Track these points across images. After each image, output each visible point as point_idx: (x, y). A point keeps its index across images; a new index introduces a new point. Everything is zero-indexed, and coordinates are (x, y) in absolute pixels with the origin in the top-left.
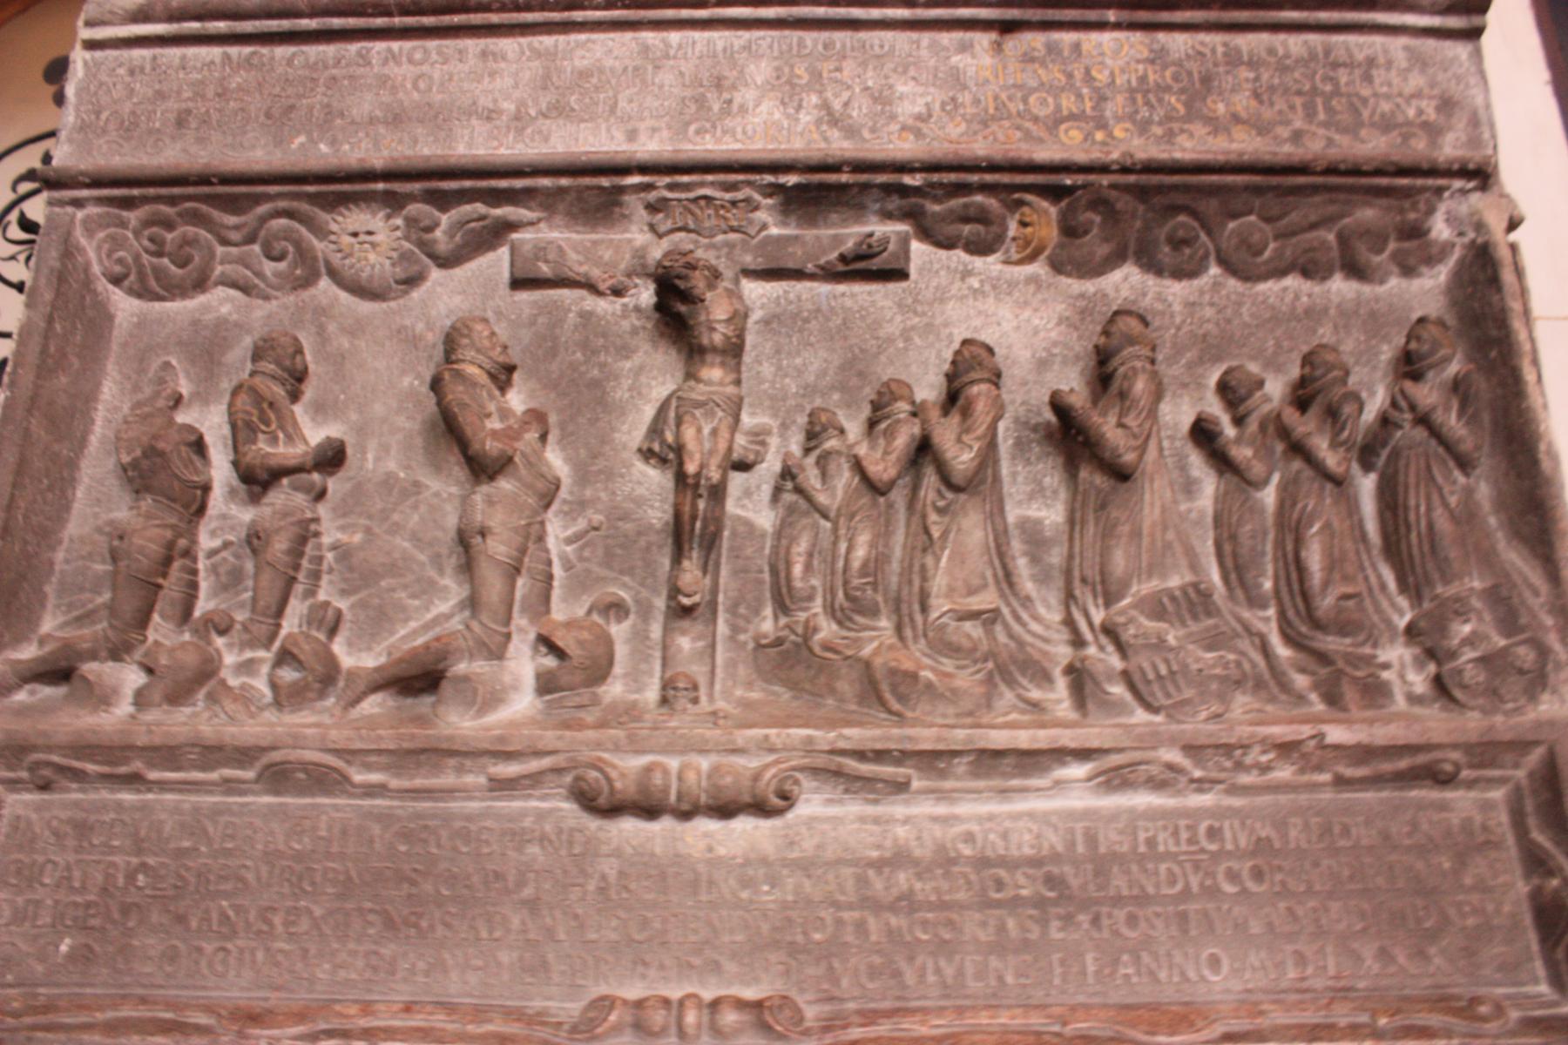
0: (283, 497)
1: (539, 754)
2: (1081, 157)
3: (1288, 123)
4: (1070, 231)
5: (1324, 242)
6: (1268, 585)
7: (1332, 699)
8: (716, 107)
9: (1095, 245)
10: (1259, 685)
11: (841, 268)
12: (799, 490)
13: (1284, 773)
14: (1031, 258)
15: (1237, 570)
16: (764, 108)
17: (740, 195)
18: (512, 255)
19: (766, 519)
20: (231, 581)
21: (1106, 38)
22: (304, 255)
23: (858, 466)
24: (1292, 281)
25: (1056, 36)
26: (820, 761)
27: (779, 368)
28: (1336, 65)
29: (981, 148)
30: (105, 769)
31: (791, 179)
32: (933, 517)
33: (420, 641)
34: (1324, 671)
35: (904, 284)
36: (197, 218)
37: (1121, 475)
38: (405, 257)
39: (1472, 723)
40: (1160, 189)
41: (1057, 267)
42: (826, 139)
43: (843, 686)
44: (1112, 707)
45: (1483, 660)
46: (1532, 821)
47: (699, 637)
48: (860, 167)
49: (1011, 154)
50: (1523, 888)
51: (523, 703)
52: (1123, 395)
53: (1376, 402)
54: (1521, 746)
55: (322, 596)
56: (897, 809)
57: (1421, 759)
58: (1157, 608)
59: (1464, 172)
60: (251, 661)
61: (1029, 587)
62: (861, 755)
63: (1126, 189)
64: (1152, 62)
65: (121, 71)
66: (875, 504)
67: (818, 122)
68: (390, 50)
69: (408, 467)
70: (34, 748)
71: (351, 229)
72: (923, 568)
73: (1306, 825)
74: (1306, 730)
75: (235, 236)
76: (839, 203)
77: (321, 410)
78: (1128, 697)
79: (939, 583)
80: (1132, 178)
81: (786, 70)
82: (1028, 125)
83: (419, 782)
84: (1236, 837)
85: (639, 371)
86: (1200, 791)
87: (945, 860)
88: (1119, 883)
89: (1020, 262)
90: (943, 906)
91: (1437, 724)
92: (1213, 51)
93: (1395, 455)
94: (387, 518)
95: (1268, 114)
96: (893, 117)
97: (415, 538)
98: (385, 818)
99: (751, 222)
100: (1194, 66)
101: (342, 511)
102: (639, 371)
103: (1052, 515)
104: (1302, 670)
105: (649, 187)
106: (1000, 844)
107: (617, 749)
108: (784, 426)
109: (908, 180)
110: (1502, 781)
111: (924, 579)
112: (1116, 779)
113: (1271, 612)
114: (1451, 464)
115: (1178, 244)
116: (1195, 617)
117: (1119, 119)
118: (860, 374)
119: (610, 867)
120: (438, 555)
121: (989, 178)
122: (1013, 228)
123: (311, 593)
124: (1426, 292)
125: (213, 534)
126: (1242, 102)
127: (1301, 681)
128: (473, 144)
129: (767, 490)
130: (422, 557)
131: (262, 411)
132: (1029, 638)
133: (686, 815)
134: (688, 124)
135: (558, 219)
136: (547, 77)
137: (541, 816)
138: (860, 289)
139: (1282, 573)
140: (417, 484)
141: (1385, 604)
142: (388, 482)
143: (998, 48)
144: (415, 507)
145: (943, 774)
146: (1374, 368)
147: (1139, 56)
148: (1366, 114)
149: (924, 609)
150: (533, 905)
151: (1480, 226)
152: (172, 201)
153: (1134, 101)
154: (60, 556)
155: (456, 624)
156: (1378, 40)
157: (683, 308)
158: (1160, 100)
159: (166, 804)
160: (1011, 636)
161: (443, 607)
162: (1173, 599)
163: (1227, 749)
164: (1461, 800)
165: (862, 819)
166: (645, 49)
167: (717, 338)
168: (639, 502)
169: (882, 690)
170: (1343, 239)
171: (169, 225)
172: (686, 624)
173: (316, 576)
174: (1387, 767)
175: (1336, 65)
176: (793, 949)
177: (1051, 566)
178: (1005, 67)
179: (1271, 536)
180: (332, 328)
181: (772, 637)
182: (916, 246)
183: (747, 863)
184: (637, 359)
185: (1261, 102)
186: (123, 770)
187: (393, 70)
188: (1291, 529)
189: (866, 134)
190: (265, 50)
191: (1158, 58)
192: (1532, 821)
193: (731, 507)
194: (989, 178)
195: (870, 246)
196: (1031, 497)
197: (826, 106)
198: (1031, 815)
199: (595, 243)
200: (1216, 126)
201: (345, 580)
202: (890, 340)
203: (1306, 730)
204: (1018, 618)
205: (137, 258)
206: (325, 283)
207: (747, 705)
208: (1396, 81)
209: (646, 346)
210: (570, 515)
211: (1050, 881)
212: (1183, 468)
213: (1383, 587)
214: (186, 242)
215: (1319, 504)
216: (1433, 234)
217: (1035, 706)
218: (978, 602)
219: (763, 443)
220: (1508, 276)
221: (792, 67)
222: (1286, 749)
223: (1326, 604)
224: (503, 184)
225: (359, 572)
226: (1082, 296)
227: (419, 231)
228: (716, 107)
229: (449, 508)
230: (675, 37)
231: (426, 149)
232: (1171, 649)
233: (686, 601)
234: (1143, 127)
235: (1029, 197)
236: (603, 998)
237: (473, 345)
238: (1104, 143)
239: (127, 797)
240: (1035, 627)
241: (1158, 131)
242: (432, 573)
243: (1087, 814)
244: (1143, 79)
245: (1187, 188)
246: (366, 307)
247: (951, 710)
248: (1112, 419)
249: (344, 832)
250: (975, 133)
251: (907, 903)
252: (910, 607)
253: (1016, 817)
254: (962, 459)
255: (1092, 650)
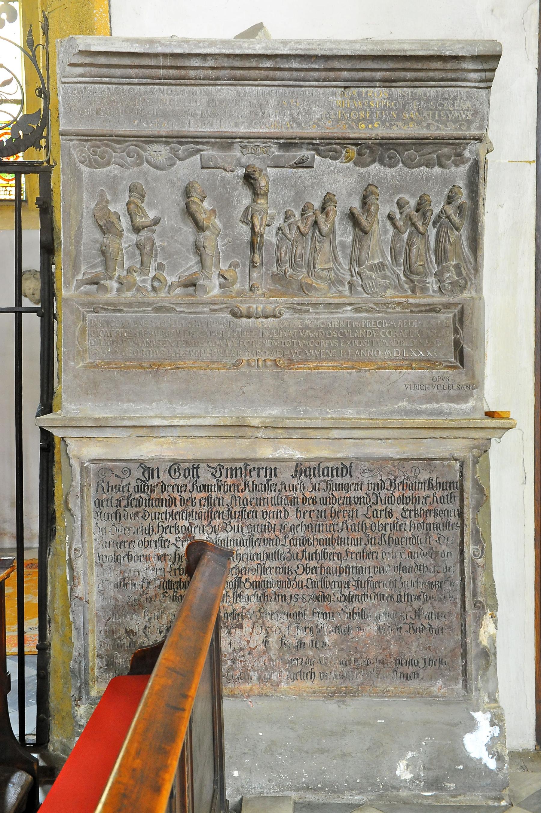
0: (144, 233)
1: (223, 304)
2: (363, 136)
3: (426, 121)
4: (360, 154)
5: (433, 158)
6: (402, 260)
7: (413, 291)
8: (260, 115)
9: (367, 157)
10: (395, 288)
11: (295, 166)
12: (282, 233)
13: (399, 309)
14: (349, 161)
15: (395, 257)
16: (274, 115)
17: (267, 145)
18: (201, 159)
19: (274, 240)
20: (132, 256)
21: (376, 89)
22: (139, 156)
23: (298, 228)
24: (423, 168)
25: (361, 89)
26: (289, 306)
27: (278, 195)
28: (445, 99)
29: (337, 132)
30: (114, 308)
31: (282, 141)
32: (317, 243)
33: (186, 274)
34: (412, 285)
35: (312, 169)
36: (107, 145)
37: (366, 233)
38: (170, 158)
39: (445, 300)
40: (385, 144)
41: (356, 164)
42: (292, 127)
43: (294, 286)
44: (358, 293)
45: (450, 283)
46: (457, 322)
47: (259, 273)
48: (301, 138)
49: (344, 135)
50: (453, 338)
51: (216, 291)
52: (368, 210)
53: (437, 210)
54: (457, 304)
55: (159, 261)
56: (307, 316)
57: (431, 307)
58: (371, 268)
59: (474, 139)
60: (145, 279)
61: (341, 260)
62: (298, 304)
63: (377, 144)
64: (389, 99)
65: (75, 92)
66: (303, 239)
67: (290, 121)
68: (160, 89)
69: (177, 223)
70: (95, 303)
71: (154, 150)
72: (314, 257)
73: (403, 321)
74: (404, 299)
75: (118, 151)
76: (295, 147)
77: (150, 205)
78: (362, 290)
79: (318, 260)
80: (378, 141)
81: (281, 102)
82: (350, 122)
83: (192, 310)
84: (386, 324)
85: (239, 195)
86: (378, 313)
87: (318, 328)
88: (357, 334)
89: (346, 162)
90: (316, 338)
91: (437, 299)
92: (408, 95)
93: (440, 225)
94: (173, 238)
95: (421, 118)
96: (311, 119)
97: (181, 244)
98: (185, 319)
99: (270, 152)
100: (401, 100)
101: (161, 236)
102: (239, 195)
103: (349, 239)
104: (407, 284)
105: (243, 142)
106: (330, 325)
107: (242, 303)
108: (279, 213)
109: (314, 142)
110: (452, 312)
111: (314, 260)
112: (358, 310)
113: (402, 268)
114: (454, 229)
115: (390, 158)
116: (380, 271)
117: (376, 120)
118: (299, 197)
119: (240, 330)
120: (188, 249)
121: (337, 141)
122: (344, 152)
123: (156, 260)
124: (459, 174)
125: (125, 243)
126: (414, 114)
127: (406, 286)
128: (190, 127)
129: (274, 231)
130: (184, 250)
131: (138, 209)
132: (340, 274)
133: (257, 318)
134: (252, 121)
135: (215, 149)
136: (209, 102)
137: (223, 318)
138: (300, 170)
139: (405, 258)
140: (180, 228)
141: (431, 267)
142: (172, 227)
143: (343, 94)
144: (180, 235)
145: (317, 309)
146: (442, 196)
147: (385, 97)
148: (450, 117)
149: (314, 268)
150: (222, 339)
151: (477, 155)
152: (100, 141)
153: (382, 113)
154: (82, 248)
155: (196, 269)
156: (459, 89)
157: (252, 181)
158: (389, 113)
159: (129, 316)
160: (335, 273)
161: (192, 263)
162: (375, 266)
163: (385, 304)
164: (442, 316)
165: (298, 318)
166: (238, 93)
167: (262, 192)
168: (241, 235)
169: (304, 288)
170: (438, 157)
171: (99, 148)
172: (255, 269)
173: (156, 255)
174: (423, 309)
175: (445, 99)
176: (282, 348)
177: (347, 254)
178: (345, 102)
179: (404, 247)
180: (149, 179)
181: (276, 273)
182: (316, 156)
183: (271, 328)
184: (239, 191)
185: (419, 114)
186: (118, 308)
187: (162, 97)
188: (410, 245)
189: (303, 126)
190: (120, 87)
191: (390, 98)
192: (457, 322)
193: (265, 236)
194: (337, 141)
195: (303, 160)
196: (343, 234)
197: (292, 115)
198: (337, 318)
199: (225, 156)
200: (405, 122)
201: (164, 256)
202: (308, 187)
203: (404, 299)
204: (337, 269)
205: (89, 156)
206: (145, 164)
207: (271, 290)
208: (462, 105)
209: (241, 188)
210: (223, 239)
211: (341, 333)
212: (384, 226)
213: (431, 262)
214: (104, 152)
215: (418, 241)
216: (465, 155)
217: (340, 292)
218: (327, 266)
219: (274, 219)
220: (481, 172)
221: (282, 101)
222: (399, 304)
223: (415, 267)
224: (200, 140)
225: (168, 255)
226: (362, 173)
227: (174, 152)
228: (260, 115)
229: (190, 235)
230: (247, 88)
231: (176, 128)
232: (373, 279)
233: (255, 265)
234: (383, 123)
235: (348, 146)
236: (240, 359)
237: (195, 191)
238: (371, 129)
239: (118, 314)
240: (342, 271)
241: (387, 124)
242: (187, 254)
243: (351, 318)
244: (385, 105)
245: (394, 144)
246: (159, 172)
247: (320, 293)
248: (365, 217)
249: (175, 322)
250: (335, 125)
251: (308, 338)
252: (311, 267)
253: (333, 318)
254: (325, 228)
255: (355, 278)
